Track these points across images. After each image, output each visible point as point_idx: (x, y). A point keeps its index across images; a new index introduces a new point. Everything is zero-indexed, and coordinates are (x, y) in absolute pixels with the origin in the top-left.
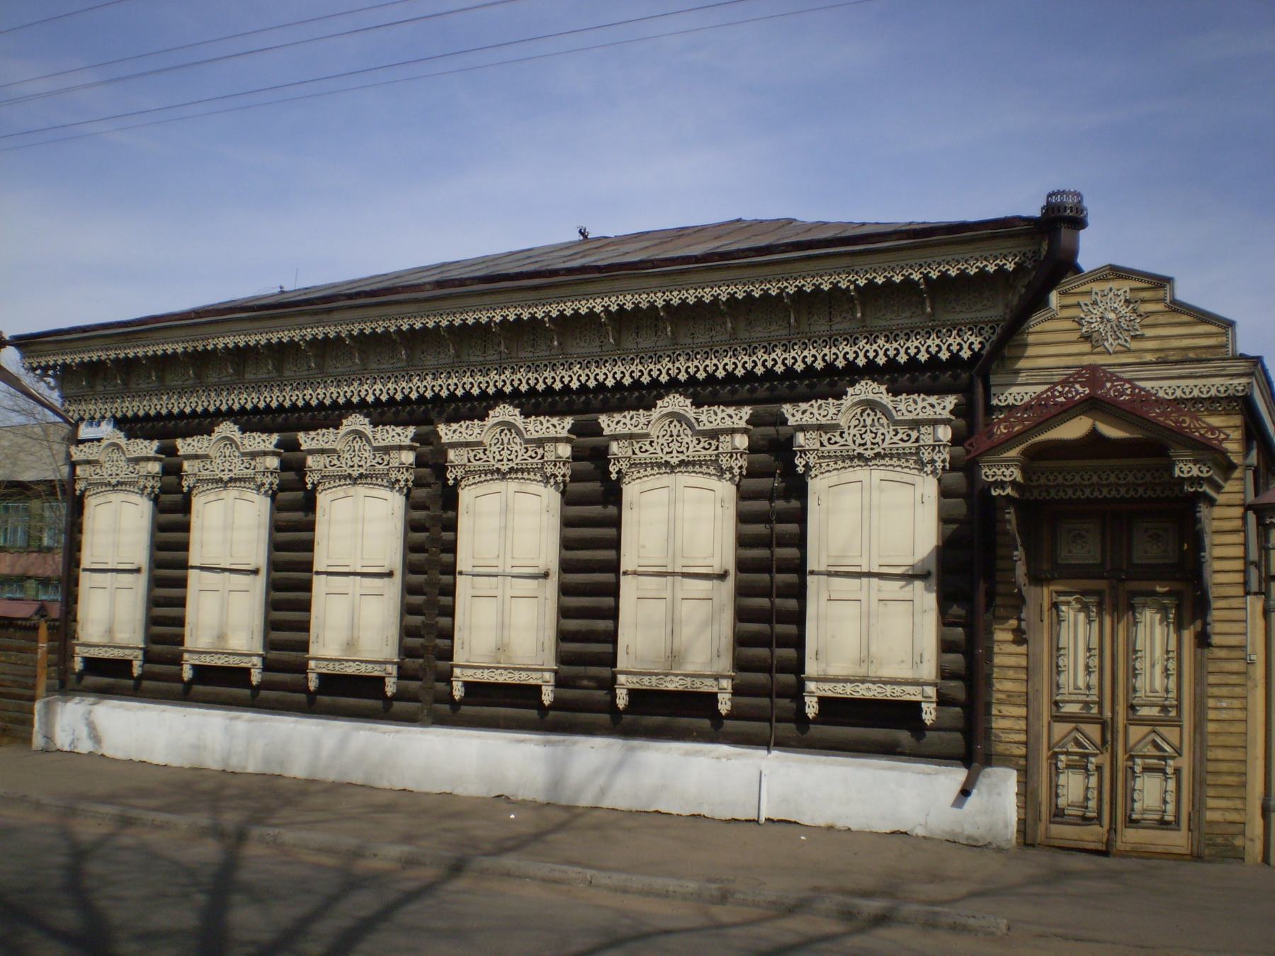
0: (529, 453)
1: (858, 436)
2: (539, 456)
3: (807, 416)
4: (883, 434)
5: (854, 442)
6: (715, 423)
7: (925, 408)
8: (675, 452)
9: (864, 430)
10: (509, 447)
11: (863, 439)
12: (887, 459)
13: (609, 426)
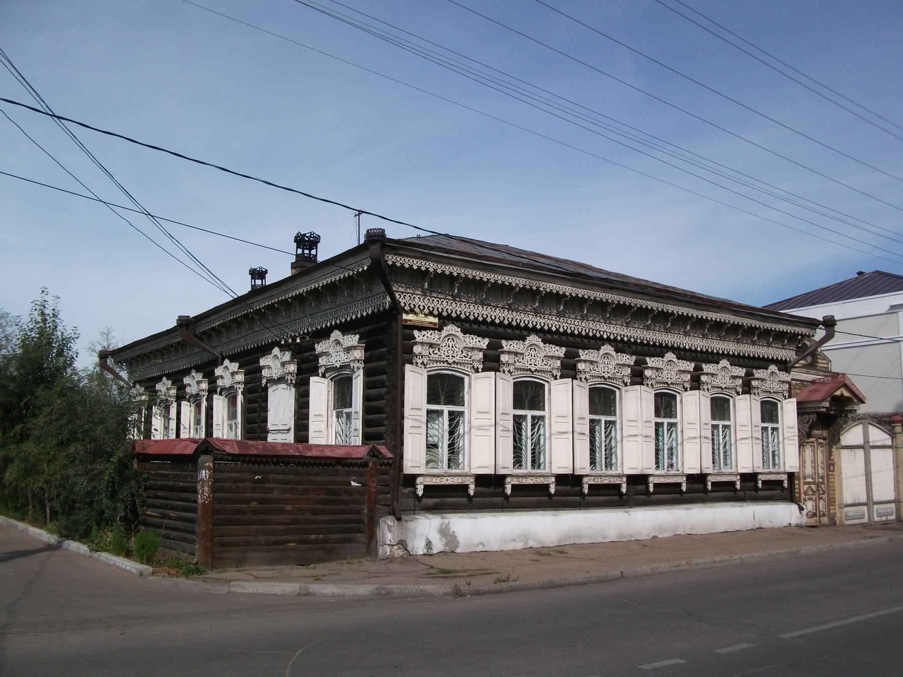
0: (545, 363)
1: (446, 351)
2: (469, 357)
3: (654, 364)
4: (457, 352)
5: (444, 354)
6: (472, 344)
7: (476, 342)
8: (533, 364)
9: (449, 348)
10: (453, 349)
11: (448, 353)
12: (459, 365)
13: (419, 336)
